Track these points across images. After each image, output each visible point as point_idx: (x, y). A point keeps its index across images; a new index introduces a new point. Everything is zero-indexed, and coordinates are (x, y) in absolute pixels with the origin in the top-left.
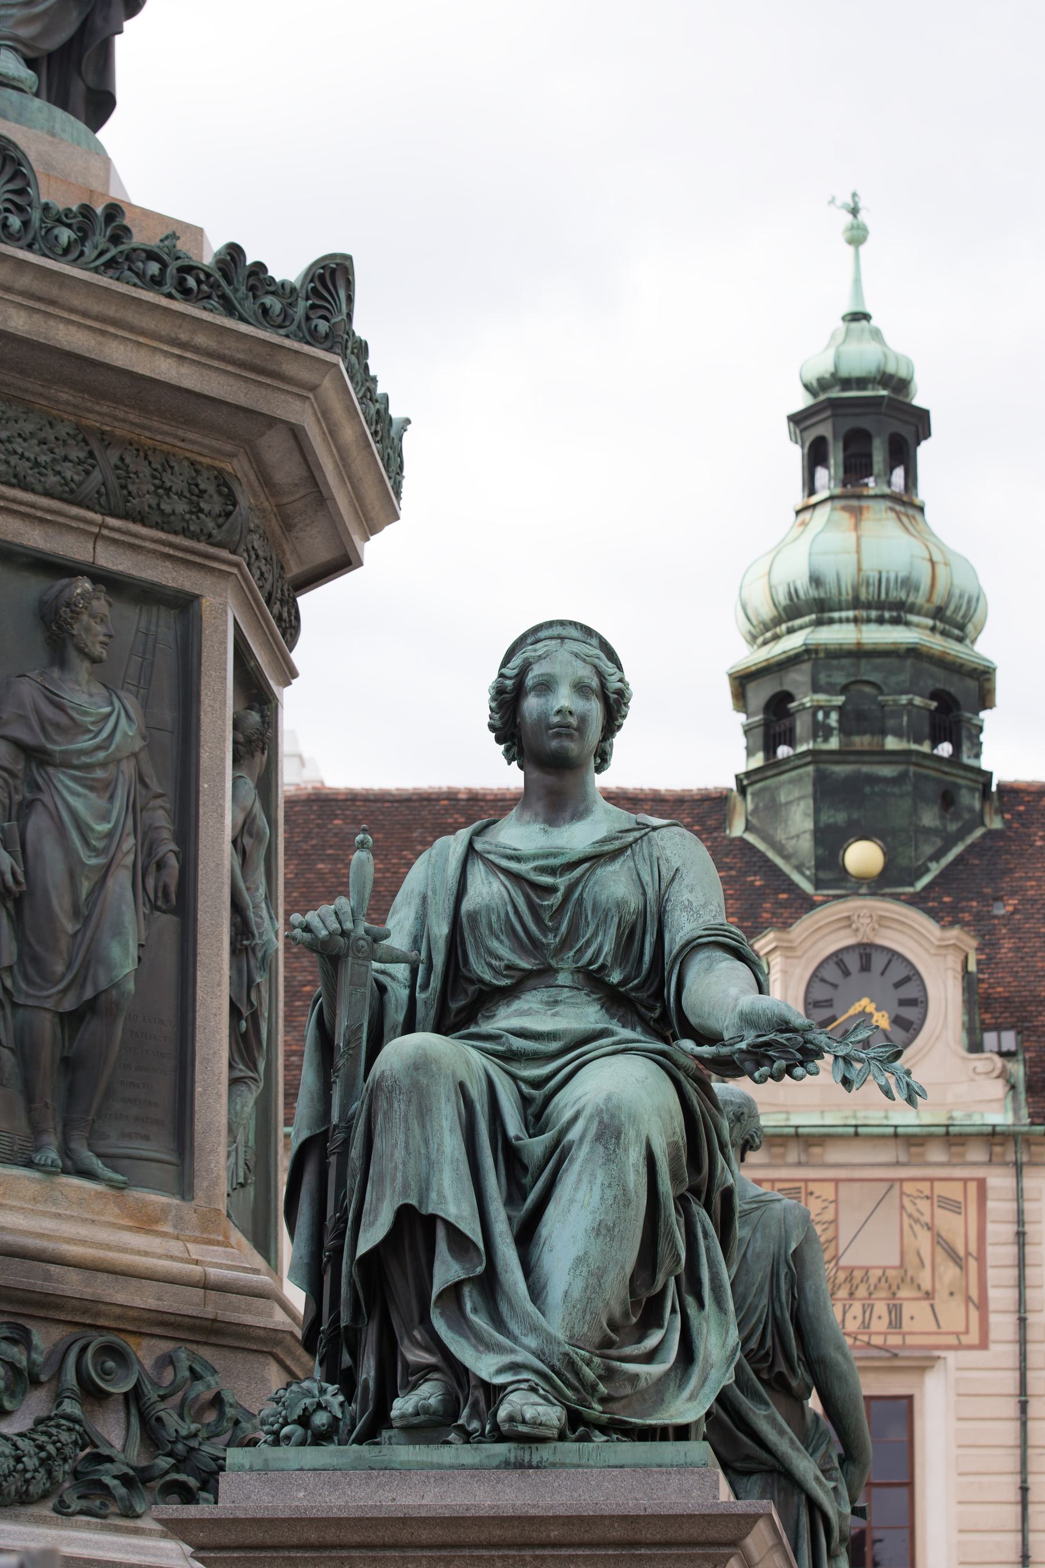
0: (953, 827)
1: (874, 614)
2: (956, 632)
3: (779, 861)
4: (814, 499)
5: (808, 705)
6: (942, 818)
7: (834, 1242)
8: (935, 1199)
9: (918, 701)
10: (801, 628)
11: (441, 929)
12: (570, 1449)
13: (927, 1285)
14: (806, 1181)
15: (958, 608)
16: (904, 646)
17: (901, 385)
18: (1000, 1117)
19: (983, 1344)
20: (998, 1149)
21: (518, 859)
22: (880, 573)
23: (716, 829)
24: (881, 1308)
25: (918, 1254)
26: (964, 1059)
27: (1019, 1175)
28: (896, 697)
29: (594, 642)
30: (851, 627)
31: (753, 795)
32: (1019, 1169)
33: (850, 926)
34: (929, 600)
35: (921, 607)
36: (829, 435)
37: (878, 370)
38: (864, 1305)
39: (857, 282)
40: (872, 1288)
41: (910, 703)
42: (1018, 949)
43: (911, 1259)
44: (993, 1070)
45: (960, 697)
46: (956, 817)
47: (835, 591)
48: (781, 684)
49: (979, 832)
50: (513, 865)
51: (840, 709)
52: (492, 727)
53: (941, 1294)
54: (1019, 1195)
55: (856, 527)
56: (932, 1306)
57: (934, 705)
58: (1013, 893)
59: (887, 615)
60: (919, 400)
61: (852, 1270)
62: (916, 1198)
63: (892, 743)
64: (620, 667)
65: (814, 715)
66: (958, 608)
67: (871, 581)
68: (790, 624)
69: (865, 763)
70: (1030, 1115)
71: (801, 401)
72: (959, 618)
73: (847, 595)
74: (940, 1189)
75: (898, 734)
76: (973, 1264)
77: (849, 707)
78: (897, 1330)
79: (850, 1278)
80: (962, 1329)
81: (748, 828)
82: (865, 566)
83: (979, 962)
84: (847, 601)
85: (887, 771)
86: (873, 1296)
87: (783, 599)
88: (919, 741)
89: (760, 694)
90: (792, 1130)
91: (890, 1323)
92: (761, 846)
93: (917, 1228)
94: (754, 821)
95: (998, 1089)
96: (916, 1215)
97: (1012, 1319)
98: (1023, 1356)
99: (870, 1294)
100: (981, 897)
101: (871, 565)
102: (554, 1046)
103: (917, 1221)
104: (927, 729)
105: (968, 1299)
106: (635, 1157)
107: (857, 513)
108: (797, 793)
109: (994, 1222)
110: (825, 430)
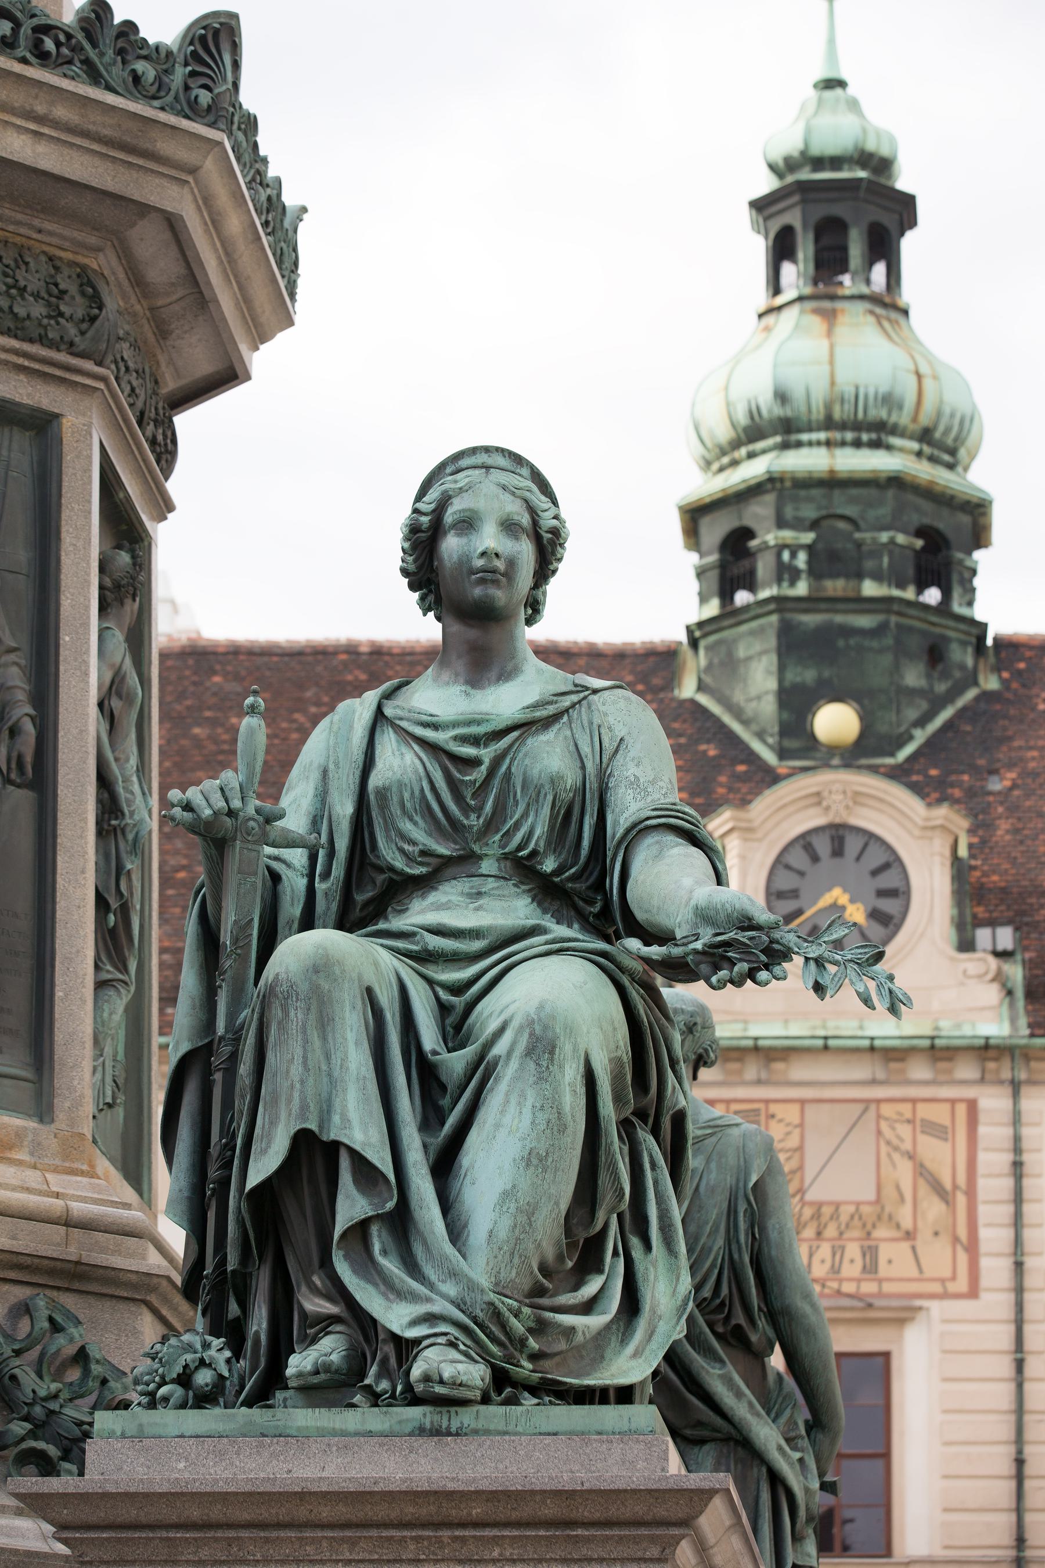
0: (941, 687)
1: (849, 436)
2: (946, 457)
3: (736, 727)
4: (780, 300)
5: (772, 543)
6: (929, 676)
7: (798, 1175)
8: (918, 1123)
9: (901, 539)
10: (764, 452)
11: (344, 808)
12: (495, 1414)
13: (907, 1223)
14: (767, 1102)
15: (948, 430)
16: (884, 475)
17: (882, 165)
19: (973, 1292)
20: (991, 1065)
21: (435, 727)
22: (857, 388)
23: (662, 689)
24: (853, 1250)
25: (898, 1188)
26: (952, 959)
27: (1016, 1095)
28: (876, 534)
29: (525, 471)
30: (823, 451)
31: (708, 649)
32: (1016, 1087)
33: (819, 803)
34: (915, 419)
35: (905, 428)
36: (798, 225)
37: (856, 148)
38: (833, 1247)
39: (831, 41)
40: (843, 1226)
41: (892, 541)
42: (1016, 831)
43: (889, 1192)
44: (986, 973)
45: (950, 534)
46: (945, 675)
47: (803, 409)
48: (740, 518)
49: (971, 694)
50: (429, 734)
51: (810, 548)
52: (405, 572)
53: (924, 1234)
54: (1016, 1119)
55: (830, 333)
56: (914, 1248)
57: (919, 543)
58: (1011, 765)
59: (865, 437)
60: (903, 183)
61: (820, 1205)
62: (896, 1121)
63: (870, 588)
64: (555, 503)
65: (779, 555)
66: (948, 430)
67: (846, 397)
68: (752, 447)
69: (836, 611)
70: (1030, 1026)
71: (765, 184)
72: (950, 441)
73: (818, 413)
74: (924, 1111)
75: (878, 577)
76: (961, 1200)
77: (820, 546)
78: (872, 1276)
79: (817, 1216)
80: (947, 1273)
81: (701, 687)
83: (971, 846)
84: (818, 421)
85: (865, 621)
86: (845, 1236)
88: (901, 585)
89: (715, 531)
90: (750, 1043)
91: (864, 1267)
92: (715, 708)
93: (896, 1156)
94: (708, 679)
95: (992, 994)
96: (895, 1141)
97: (1005, 1265)
98: (1019, 1307)
99: (841, 1234)
100: (974, 770)
101: (846, 381)
102: (477, 945)
103: (896, 1149)
104: (911, 572)
105: (956, 1240)
106: (571, 1075)
107: (830, 317)
108: (757, 647)
109: (986, 1150)
110: (794, 218)
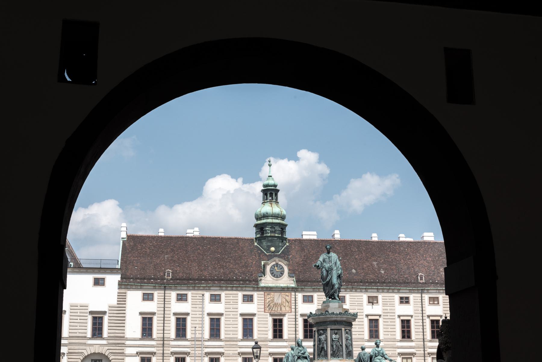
0: (283, 245)
1: (274, 218)
3: (262, 249)
6: (282, 244)
10: (265, 219)
13: (285, 305)
18: (293, 285)
19: (291, 312)
24: (279, 308)
30: (271, 220)
42: (292, 262)
43: (283, 302)
46: (283, 244)
49: (286, 246)
51: (270, 230)
53: (286, 306)
55: (272, 206)
58: (291, 254)
60: (277, 188)
63: (276, 235)
75: (277, 234)
76: (290, 303)
82: (273, 212)
85: (276, 239)
88: (279, 235)
95: (293, 282)
97: (294, 309)
107: (271, 204)
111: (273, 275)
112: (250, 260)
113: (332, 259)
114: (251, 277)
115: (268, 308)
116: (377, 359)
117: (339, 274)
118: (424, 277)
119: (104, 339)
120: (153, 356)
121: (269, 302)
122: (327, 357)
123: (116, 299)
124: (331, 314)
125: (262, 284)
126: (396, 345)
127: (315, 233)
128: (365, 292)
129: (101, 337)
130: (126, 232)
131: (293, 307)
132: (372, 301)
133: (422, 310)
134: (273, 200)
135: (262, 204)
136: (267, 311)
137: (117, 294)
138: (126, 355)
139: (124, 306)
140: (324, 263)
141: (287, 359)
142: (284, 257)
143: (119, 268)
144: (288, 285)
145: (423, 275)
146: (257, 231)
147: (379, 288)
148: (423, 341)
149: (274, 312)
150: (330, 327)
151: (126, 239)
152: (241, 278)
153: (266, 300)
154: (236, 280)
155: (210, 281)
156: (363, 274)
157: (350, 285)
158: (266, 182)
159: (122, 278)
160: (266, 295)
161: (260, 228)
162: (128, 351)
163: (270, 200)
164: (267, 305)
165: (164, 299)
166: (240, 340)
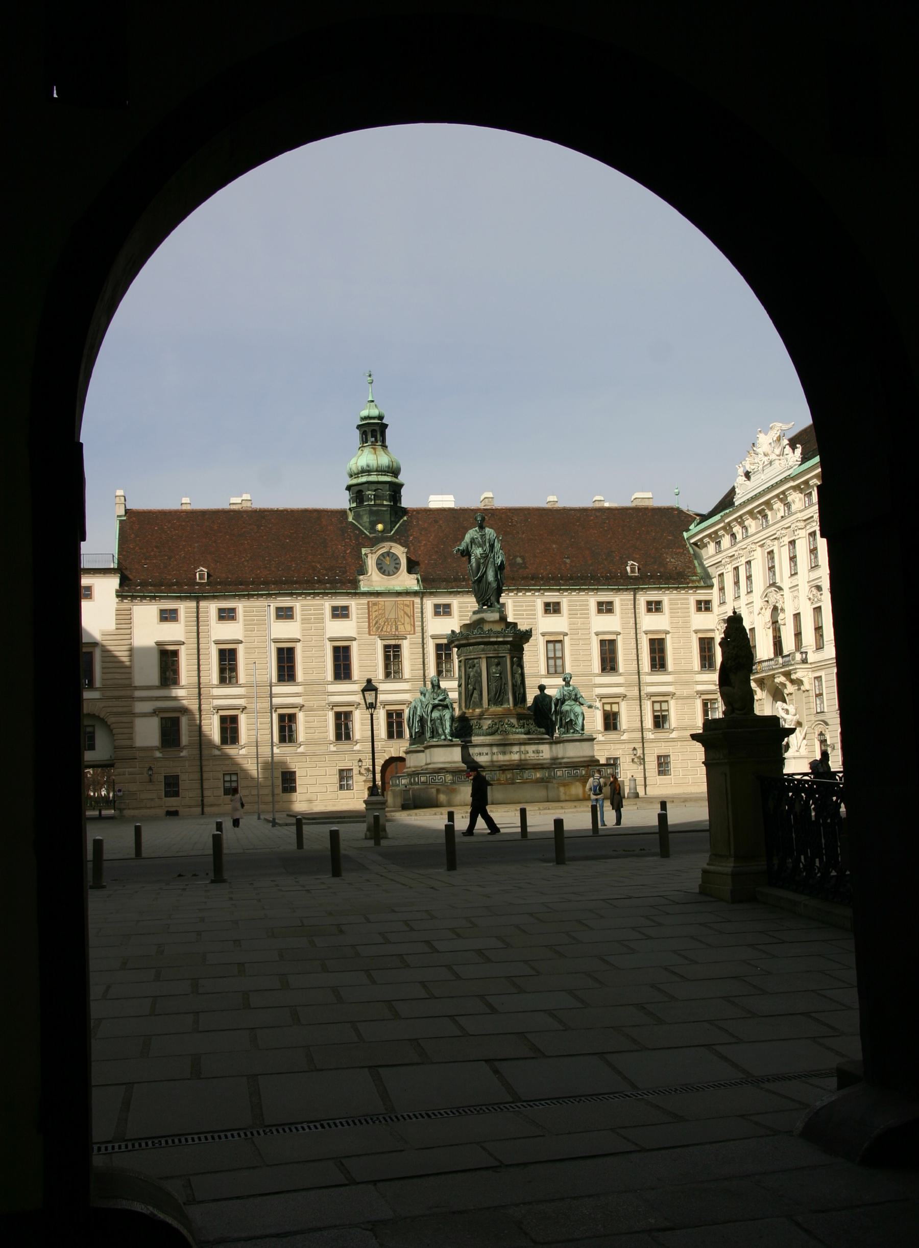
0: (397, 520)
1: (380, 473)
3: (361, 527)
18: (416, 588)
19: (414, 634)
24: (394, 627)
30: (376, 476)
42: (414, 549)
43: (399, 616)
47: (372, 468)
49: (402, 521)
51: (374, 495)
55: (375, 453)
57: (393, 493)
58: (411, 536)
59: (383, 473)
60: (384, 421)
63: (385, 503)
68: (362, 474)
70: (423, 587)
75: (386, 500)
76: (412, 618)
80: (410, 630)
81: (353, 519)
87: (360, 469)
92: (357, 524)
107: (374, 449)
111: (383, 570)
112: (341, 546)
113: (487, 537)
114: (344, 576)
115: (375, 628)
116: (567, 705)
117: (499, 564)
118: (637, 567)
119: (97, 689)
120: (184, 714)
121: (376, 617)
122: (481, 704)
123: (114, 621)
124: (487, 632)
125: (363, 588)
126: (593, 683)
127: (451, 498)
128: (538, 596)
129: (93, 688)
130: (124, 505)
131: (418, 623)
132: (552, 608)
133: (636, 624)
134: (377, 442)
135: (359, 448)
136: (374, 633)
137: (114, 613)
138: (137, 715)
139: (128, 631)
140: (473, 546)
141: (414, 711)
142: (399, 539)
143: (116, 567)
144: (408, 587)
145: (635, 564)
146: (353, 497)
147: (563, 587)
148: (637, 674)
149: (385, 633)
150: (486, 654)
151: (125, 518)
152: (326, 578)
153: (371, 614)
154: (319, 581)
155: (274, 584)
156: (535, 566)
157: (512, 585)
158: (365, 413)
159: (121, 585)
160: (370, 605)
161: (357, 493)
162: (140, 707)
163: (372, 442)
164: (374, 622)
165: (198, 617)
166: (330, 683)
